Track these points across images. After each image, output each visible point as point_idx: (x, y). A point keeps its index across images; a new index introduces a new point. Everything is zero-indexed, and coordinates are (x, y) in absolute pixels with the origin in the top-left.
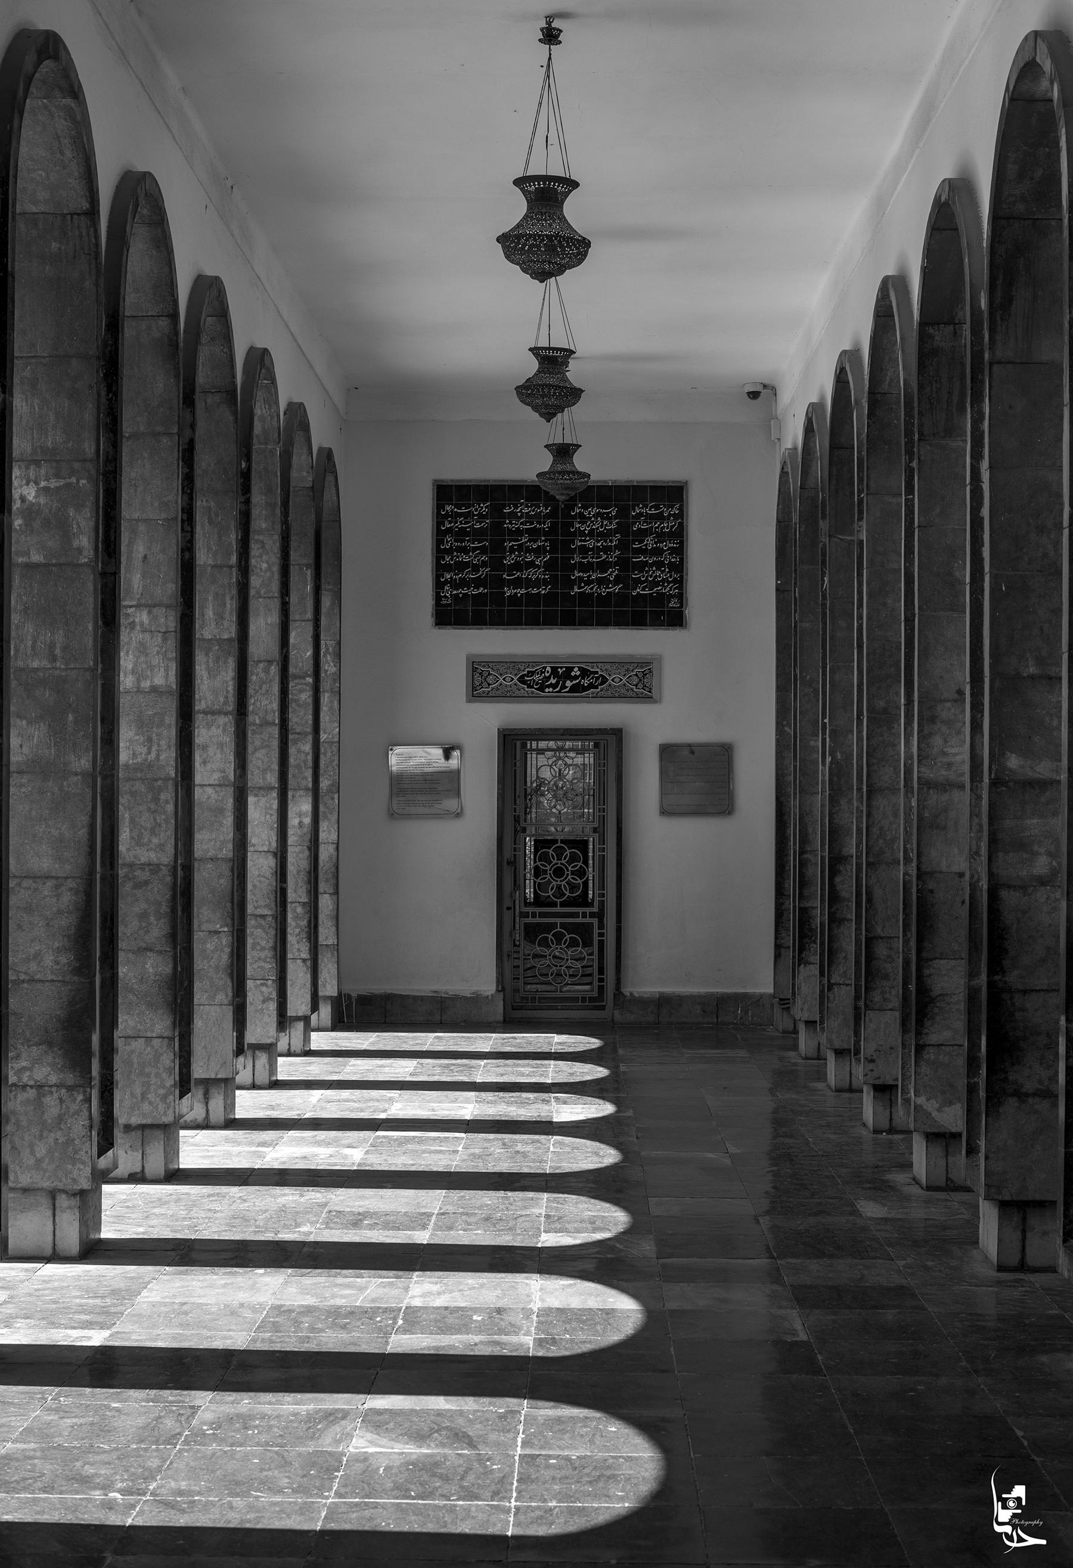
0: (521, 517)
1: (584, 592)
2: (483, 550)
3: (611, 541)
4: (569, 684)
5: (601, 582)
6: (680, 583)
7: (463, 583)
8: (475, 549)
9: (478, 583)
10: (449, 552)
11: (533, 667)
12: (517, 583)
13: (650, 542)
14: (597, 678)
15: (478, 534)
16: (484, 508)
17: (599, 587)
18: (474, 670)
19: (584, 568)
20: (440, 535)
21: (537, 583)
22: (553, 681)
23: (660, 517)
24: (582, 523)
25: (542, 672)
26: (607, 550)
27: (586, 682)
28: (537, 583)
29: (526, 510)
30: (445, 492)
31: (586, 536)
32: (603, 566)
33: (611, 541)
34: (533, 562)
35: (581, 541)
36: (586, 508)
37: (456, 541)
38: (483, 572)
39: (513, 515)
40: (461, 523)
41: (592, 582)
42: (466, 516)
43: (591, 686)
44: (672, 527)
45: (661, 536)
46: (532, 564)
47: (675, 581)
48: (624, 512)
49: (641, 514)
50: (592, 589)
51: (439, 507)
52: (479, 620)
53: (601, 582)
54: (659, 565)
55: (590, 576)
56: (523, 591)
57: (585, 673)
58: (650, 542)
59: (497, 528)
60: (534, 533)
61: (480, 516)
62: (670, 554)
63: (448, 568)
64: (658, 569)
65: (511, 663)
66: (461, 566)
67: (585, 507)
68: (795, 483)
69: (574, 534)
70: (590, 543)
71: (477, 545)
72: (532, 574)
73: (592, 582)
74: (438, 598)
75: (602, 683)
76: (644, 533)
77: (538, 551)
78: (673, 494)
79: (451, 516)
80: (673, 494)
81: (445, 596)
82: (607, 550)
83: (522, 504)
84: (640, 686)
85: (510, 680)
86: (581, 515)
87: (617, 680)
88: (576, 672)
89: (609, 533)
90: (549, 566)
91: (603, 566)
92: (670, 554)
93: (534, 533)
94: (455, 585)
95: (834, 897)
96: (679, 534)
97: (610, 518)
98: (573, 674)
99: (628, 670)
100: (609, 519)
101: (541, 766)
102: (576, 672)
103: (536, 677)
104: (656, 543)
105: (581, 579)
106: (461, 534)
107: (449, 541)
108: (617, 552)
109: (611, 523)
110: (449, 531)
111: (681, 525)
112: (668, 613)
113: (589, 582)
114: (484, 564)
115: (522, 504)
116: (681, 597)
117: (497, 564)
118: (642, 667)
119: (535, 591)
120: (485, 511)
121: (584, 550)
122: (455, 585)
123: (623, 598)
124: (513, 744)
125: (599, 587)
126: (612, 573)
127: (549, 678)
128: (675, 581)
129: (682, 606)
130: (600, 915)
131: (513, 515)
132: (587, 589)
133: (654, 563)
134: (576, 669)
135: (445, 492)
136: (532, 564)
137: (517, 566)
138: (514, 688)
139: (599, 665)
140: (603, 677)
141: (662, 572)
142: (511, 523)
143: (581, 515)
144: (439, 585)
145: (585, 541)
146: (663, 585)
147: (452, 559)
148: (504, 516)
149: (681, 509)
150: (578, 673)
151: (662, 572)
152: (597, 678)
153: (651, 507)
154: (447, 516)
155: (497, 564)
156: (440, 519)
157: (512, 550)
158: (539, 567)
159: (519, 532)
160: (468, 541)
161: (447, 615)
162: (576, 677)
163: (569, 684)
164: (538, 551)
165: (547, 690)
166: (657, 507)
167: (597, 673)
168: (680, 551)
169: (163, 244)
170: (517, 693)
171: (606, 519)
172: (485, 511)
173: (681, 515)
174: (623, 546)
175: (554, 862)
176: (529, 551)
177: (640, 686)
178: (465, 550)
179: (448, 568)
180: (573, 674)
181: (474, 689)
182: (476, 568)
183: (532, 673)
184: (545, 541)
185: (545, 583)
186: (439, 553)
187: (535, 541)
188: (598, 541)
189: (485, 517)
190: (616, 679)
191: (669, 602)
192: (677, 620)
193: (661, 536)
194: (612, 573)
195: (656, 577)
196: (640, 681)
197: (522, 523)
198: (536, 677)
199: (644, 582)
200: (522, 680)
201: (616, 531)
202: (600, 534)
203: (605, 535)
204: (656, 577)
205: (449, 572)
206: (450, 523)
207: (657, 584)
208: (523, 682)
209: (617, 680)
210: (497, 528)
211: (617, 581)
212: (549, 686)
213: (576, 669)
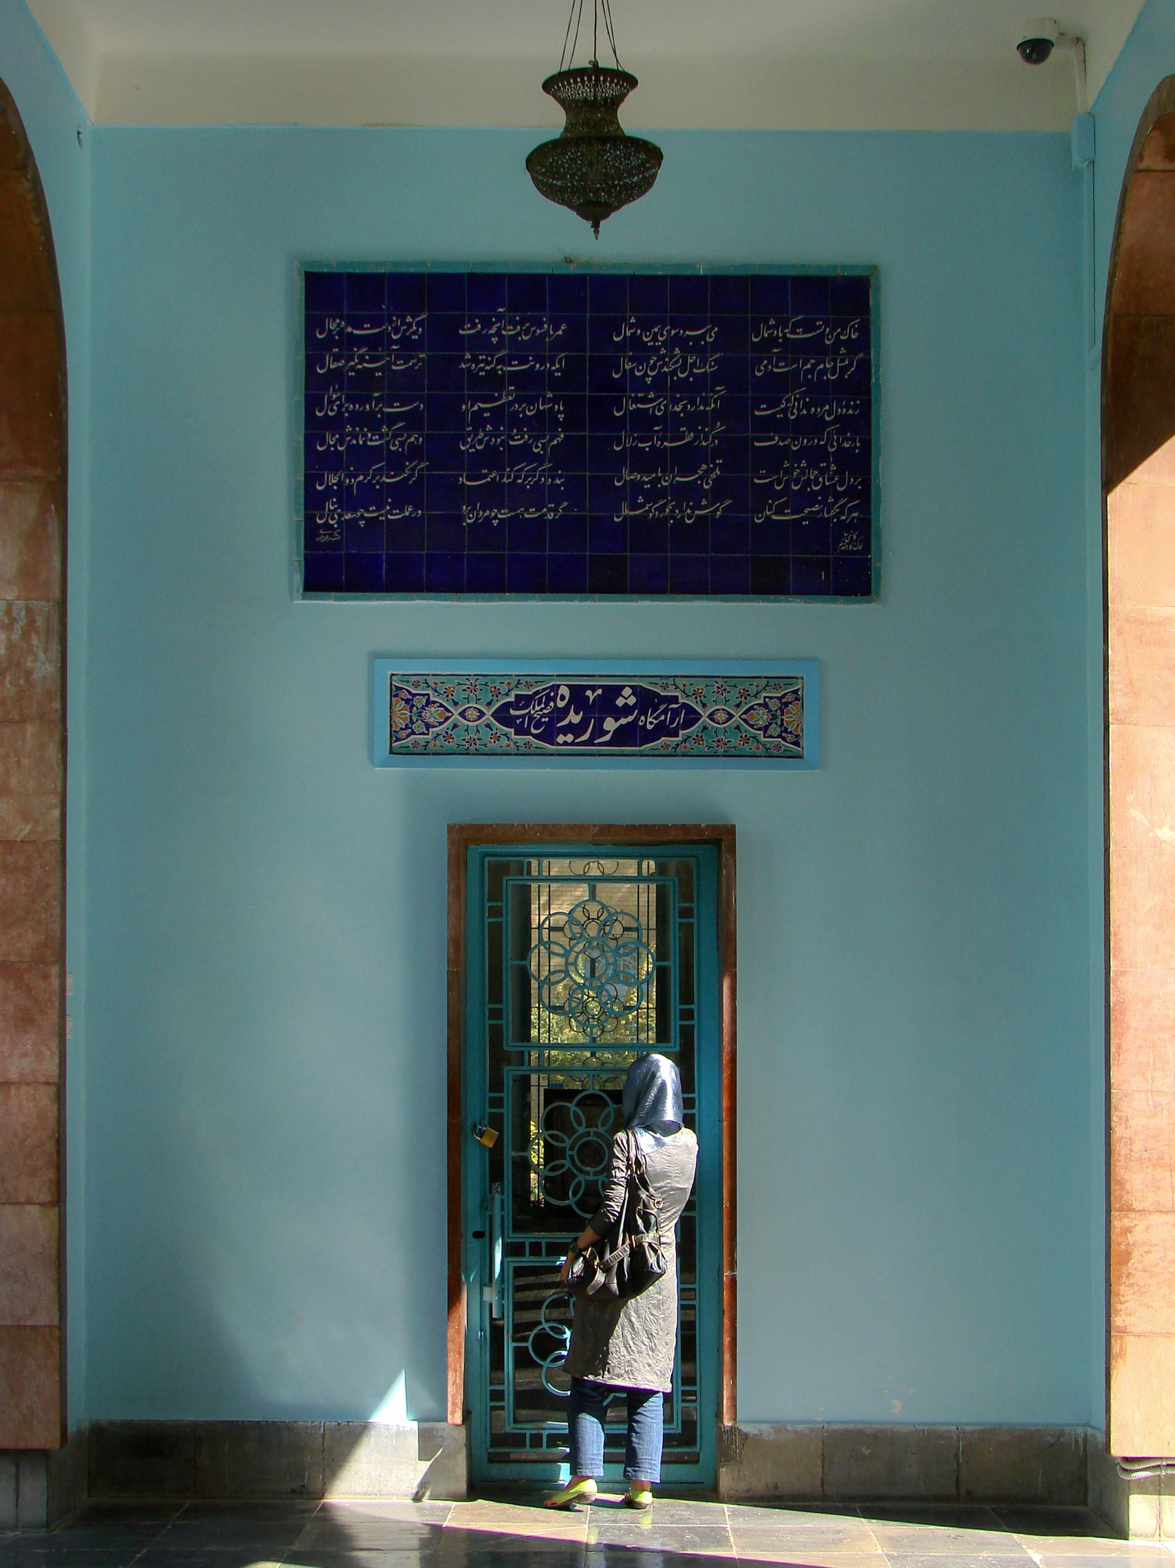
0: (498, 347)
1: (644, 517)
2: (413, 421)
3: (705, 402)
4: (610, 725)
5: (683, 493)
6: (863, 495)
8: (392, 419)
9: (401, 495)
10: (334, 424)
11: (529, 685)
12: (492, 495)
13: (793, 406)
14: (676, 713)
16: (414, 325)
17: (679, 506)
18: (395, 692)
19: (642, 461)
21: (538, 496)
22: (574, 718)
23: (815, 348)
24: (639, 360)
25: (549, 699)
26: (694, 420)
27: (649, 722)
28: (538, 496)
29: (509, 332)
31: (646, 388)
32: (688, 459)
33: (705, 402)
34: (526, 447)
35: (636, 400)
36: (646, 328)
37: (350, 399)
38: (414, 470)
39: (480, 342)
40: (362, 359)
41: (662, 493)
42: (373, 342)
43: (662, 730)
44: (844, 370)
45: (818, 391)
46: (524, 454)
47: (851, 493)
49: (772, 341)
50: (662, 509)
51: (312, 323)
53: (683, 493)
54: (815, 456)
55: (658, 480)
56: (505, 514)
57: (647, 700)
58: (793, 406)
60: (529, 384)
61: (405, 342)
62: (840, 432)
63: (331, 461)
64: (813, 465)
65: (477, 684)
66: (362, 457)
67: (646, 326)
69: (619, 386)
70: (657, 407)
71: (396, 409)
72: (524, 475)
73: (662, 493)
74: (311, 531)
75: (688, 724)
76: (775, 387)
77: (541, 424)
78: (844, 298)
79: (338, 344)
80: (844, 298)
81: (327, 526)
82: (694, 420)
83: (500, 318)
84: (774, 730)
85: (480, 723)
86: (635, 341)
87: (720, 716)
88: (627, 698)
89: (699, 385)
90: (562, 458)
91: (688, 459)
92: (840, 432)
93: (529, 384)
94: (347, 499)
96: (858, 389)
97: (703, 350)
98: (620, 702)
99: (745, 694)
100: (698, 348)
102: (627, 698)
103: (536, 710)
104: (807, 406)
105: (636, 487)
106: (360, 386)
107: (335, 402)
108: (720, 428)
109: (704, 361)
110: (336, 375)
111: (865, 367)
112: (839, 562)
113: (654, 494)
114: (415, 452)
115: (499, 319)
116: (864, 528)
118: (777, 688)
119: (532, 514)
120: (416, 332)
121: (643, 422)
122: (347, 499)
125: (679, 506)
126: (708, 475)
127: (565, 712)
128: (851, 493)
129: (867, 549)
131: (480, 342)
132: (651, 510)
133: (804, 452)
134: (627, 692)
136: (524, 454)
137: (491, 458)
138: (485, 734)
139: (679, 682)
140: (690, 710)
141: (823, 471)
142: (475, 360)
143: (635, 341)
144: (313, 501)
145: (645, 400)
146: (824, 502)
147: (341, 442)
148: (460, 343)
149: (865, 330)
150: (632, 701)
151: (823, 471)
152: (676, 713)
153: (796, 325)
154: (329, 343)
157: (478, 420)
158: (539, 459)
159: (495, 382)
160: (379, 400)
161: (335, 566)
162: (627, 710)
163: (610, 725)
164: (541, 424)
165: (561, 739)
166: (808, 326)
167: (675, 699)
168: (861, 424)
170: (493, 746)
171: (692, 351)
172: (416, 332)
173: (864, 343)
175: (581, 1130)
176: (516, 422)
177: (774, 730)
178: (371, 422)
179: (331, 461)
180: (620, 702)
181: (394, 736)
182: (396, 462)
183: (524, 701)
184: (555, 400)
185: (555, 495)
186: (315, 427)
187: (531, 401)
188: (676, 402)
189: (418, 346)
191: (838, 539)
193: (818, 391)
194: (708, 475)
195: (808, 483)
196: (773, 721)
197: (500, 361)
198: (536, 710)
199: (781, 494)
200: (502, 715)
201: (716, 379)
202: (680, 386)
203: (695, 387)
204: (808, 483)
205: (334, 469)
206: (337, 358)
207: (812, 499)
208: (507, 721)
209: (720, 716)
211: (717, 494)
212: (565, 730)
213: (627, 692)
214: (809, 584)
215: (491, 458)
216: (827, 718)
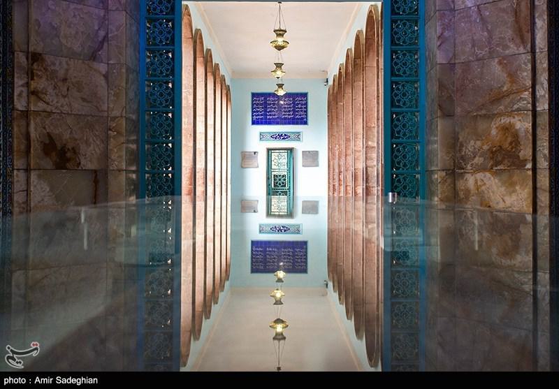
6: (306, 115)
7: (258, 115)
9: (261, 115)
13: (300, 106)
15: (261, 104)
16: (263, 98)
20: (253, 105)
28: (275, 115)
30: (254, 95)
32: (289, 111)
45: (302, 105)
48: (294, 99)
52: (262, 123)
57: (285, 135)
58: (300, 106)
59: (265, 103)
63: (255, 112)
66: (258, 111)
68: (331, 91)
70: (286, 106)
72: (273, 113)
78: (305, 95)
80: (305, 95)
85: (269, 136)
91: (289, 111)
95: (339, 180)
101: (274, 155)
117: (266, 111)
123: (293, 118)
124: (269, 150)
126: (291, 113)
130: (289, 189)
135: (254, 95)
137: (270, 111)
155: (266, 111)
156: (253, 101)
159: (271, 104)
161: (253, 123)
164: (275, 108)
169: (202, 43)
174: (294, 107)
178: (258, 108)
179: (255, 112)
186: (253, 109)
190: (292, 136)
192: (306, 123)
193: (302, 105)
194: (291, 113)
196: (298, 137)
210: (265, 103)
214: (301, 123)
215: (270, 111)
216: (304, 137)
